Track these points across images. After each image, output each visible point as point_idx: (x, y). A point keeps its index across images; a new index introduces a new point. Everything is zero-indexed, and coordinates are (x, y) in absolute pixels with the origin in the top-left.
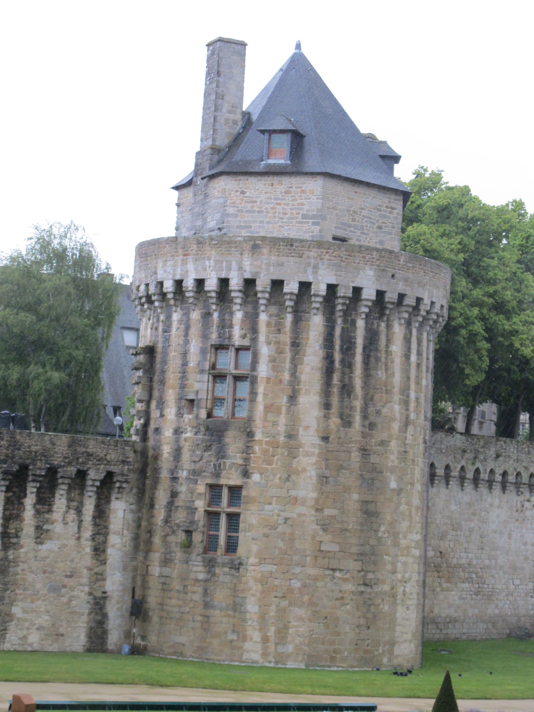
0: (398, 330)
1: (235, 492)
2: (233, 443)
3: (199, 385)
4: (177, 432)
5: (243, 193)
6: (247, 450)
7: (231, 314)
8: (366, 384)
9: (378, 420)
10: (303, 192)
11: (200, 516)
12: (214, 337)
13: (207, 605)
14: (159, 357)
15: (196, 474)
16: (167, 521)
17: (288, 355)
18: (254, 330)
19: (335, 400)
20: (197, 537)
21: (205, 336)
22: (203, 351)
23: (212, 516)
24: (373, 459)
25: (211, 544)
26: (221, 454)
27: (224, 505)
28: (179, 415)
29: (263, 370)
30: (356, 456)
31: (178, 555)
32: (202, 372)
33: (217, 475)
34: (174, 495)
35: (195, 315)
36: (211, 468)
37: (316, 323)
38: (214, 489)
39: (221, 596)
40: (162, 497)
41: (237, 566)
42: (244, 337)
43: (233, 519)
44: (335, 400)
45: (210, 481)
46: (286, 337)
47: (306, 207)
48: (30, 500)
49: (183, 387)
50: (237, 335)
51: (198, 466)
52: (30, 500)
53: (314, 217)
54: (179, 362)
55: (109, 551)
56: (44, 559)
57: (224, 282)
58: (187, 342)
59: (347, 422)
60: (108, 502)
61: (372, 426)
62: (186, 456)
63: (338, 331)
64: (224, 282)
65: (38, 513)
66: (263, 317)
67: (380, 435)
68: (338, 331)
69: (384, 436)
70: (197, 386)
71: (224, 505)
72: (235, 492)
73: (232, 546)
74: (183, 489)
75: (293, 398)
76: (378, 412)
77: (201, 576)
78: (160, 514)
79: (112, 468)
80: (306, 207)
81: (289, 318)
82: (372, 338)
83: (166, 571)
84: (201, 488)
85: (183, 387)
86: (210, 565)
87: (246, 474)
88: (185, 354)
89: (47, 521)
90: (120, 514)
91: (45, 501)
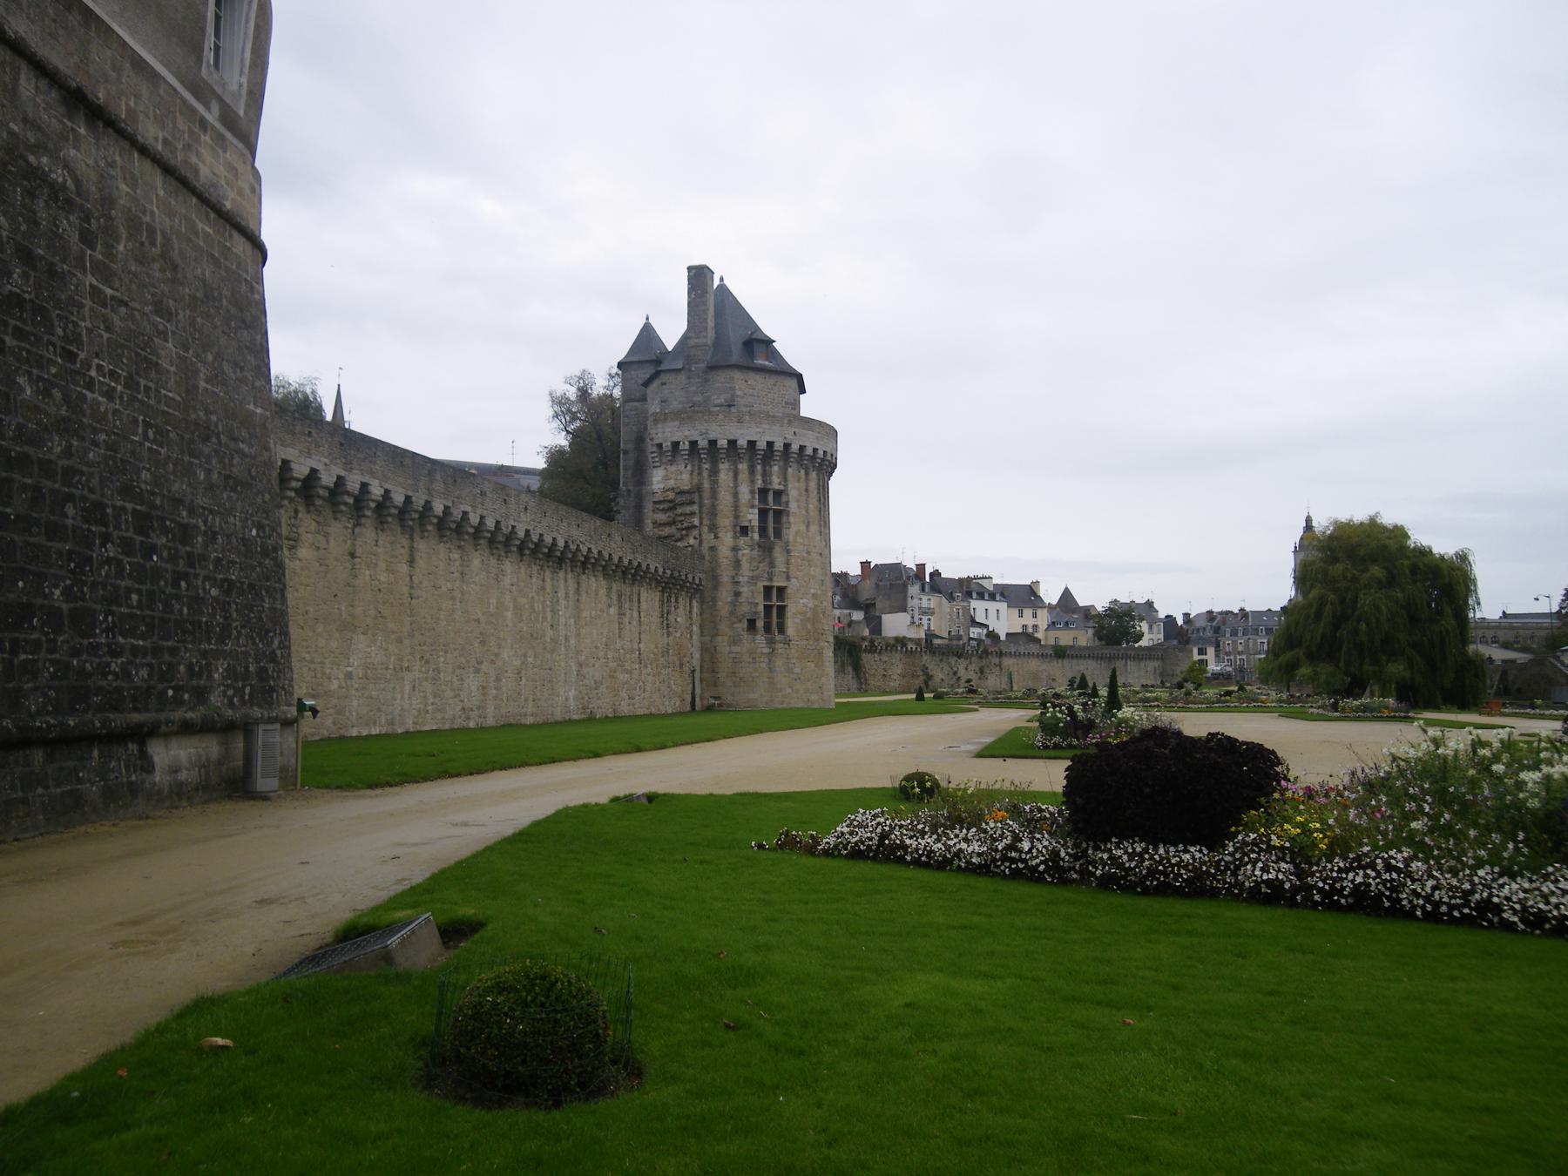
1: (781, 590)
2: (778, 554)
3: (752, 517)
4: (735, 549)
6: (788, 563)
11: (761, 608)
12: (759, 483)
13: (771, 670)
15: (754, 580)
16: (732, 614)
18: (785, 479)
20: (760, 624)
21: (753, 482)
22: (752, 492)
23: (768, 608)
25: (768, 628)
26: (772, 565)
27: (774, 601)
28: (735, 537)
29: (793, 506)
31: (746, 636)
32: (753, 507)
33: (771, 580)
34: (737, 594)
35: (743, 467)
38: (768, 590)
39: (779, 663)
40: (725, 595)
41: (787, 642)
43: (782, 610)
46: (802, 485)
49: (736, 517)
50: (776, 483)
57: (770, 444)
58: (736, 486)
62: (745, 564)
64: (770, 444)
71: (774, 601)
72: (781, 590)
73: (782, 630)
74: (745, 590)
75: (808, 527)
77: (766, 650)
78: (723, 608)
83: (736, 649)
85: (736, 517)
86: (771, 642)
87: (788, 578)
88: (736, 495)
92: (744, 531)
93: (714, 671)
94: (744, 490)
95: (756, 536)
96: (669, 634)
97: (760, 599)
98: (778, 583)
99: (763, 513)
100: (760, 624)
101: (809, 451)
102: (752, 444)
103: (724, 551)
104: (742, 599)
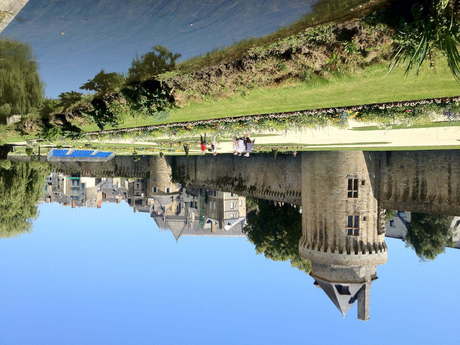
0: (309, 240)
1: (350, 195)
3: (362, 224)
5: (354, 278)
7: (354, 245)
8: (316, 225)
9: (313, 215)
10: (337, 277)
11: (359, 189)
14: (376, 232)
17: (337, 233)
19: (324, 221)
22: (362, 234)
23: (356, 188)
24: (313, 205)
25: (356, 181)
26: (354, 206)
30: (317, 206)
32: (362, 229)
36: (357, 202)
37: (330, 242)
38: (356, 195)
42: (350, 238)
43: (350, 188)
44: (324, 221)
45: (357, 199)
46: (338, 238)
47: (335, 273)
48: (411, 192)
51: (361, 203)
52: (411, 192)
53: (333, 270)
54: (369, 231)
55: (387, 178)
56: (406, 175)
57: (356, 253)
59: (320, 215)
60: (388, 192)
61: (314, 214)
62: (365, 206)
63: (324, 239)
64: (356, 253)
65: (408, 189)
66: (344, 244)
67: (312, 212)
68: (324, 239)
69: (311, 211)
70: (363, 224)
72: (350, 195)
73: (350, 181)
74: (365, 196)
76: (313, 217)
79: (387, 201)
80: (335, 273)
81: (337, 243)
82: (315, 237)
84: (359, 196)
89: (405, 186)
90: (385, 188)
91: (406, 192)
92: (365, 219)
93: (376, 165)
94: (364, 234)
95: (360, 217)
96: (417, 178)
97: (360, 192)
98: (352, 199)
99: (357, 225)
100: (360, 183)
101: (337, 252)
102: (364, 253)
103: (371, 210)
104: (366, 192)
